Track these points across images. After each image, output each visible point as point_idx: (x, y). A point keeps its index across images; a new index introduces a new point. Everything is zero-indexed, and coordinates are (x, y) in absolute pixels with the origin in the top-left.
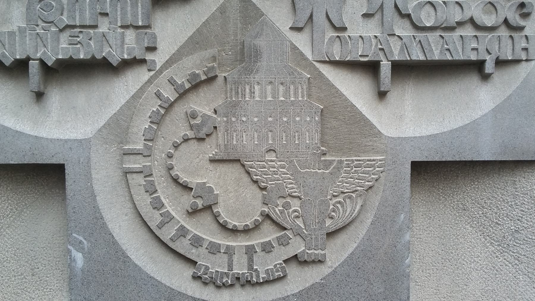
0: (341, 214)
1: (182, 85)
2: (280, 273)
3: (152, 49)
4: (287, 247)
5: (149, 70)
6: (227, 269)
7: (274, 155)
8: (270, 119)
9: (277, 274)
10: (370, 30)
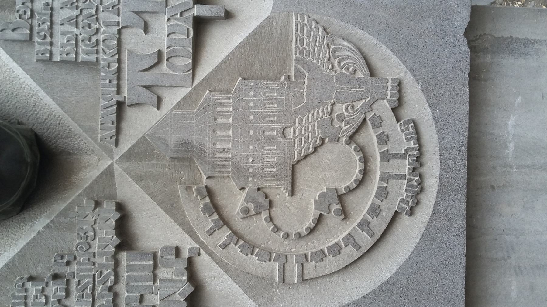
0: (351, 61)
1: (215, 221)
2: (410, 126)
3: (178, 252)
4: (383, 118)
5: (199, 254)
6: (404, 181)
7: (288, 129)
8: (251, 133)
9: (411, 130)
10: (161, 25)
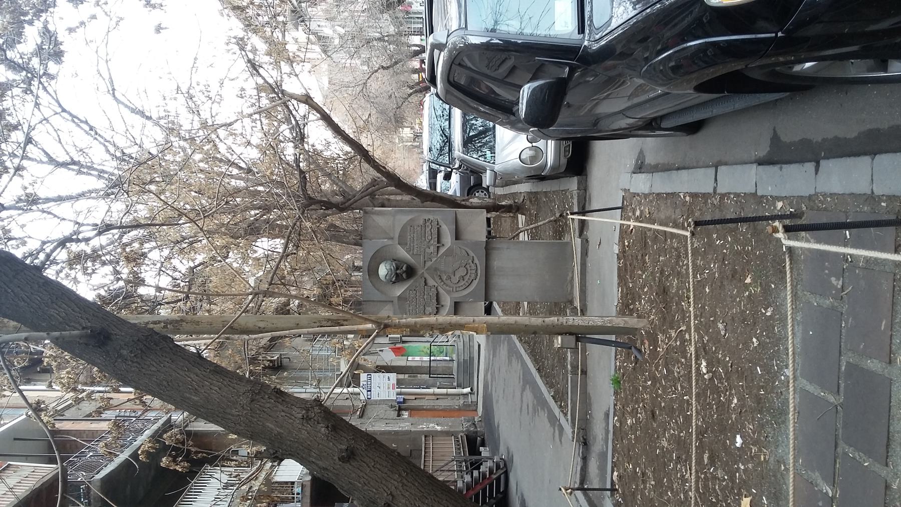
10: (432, 248)
